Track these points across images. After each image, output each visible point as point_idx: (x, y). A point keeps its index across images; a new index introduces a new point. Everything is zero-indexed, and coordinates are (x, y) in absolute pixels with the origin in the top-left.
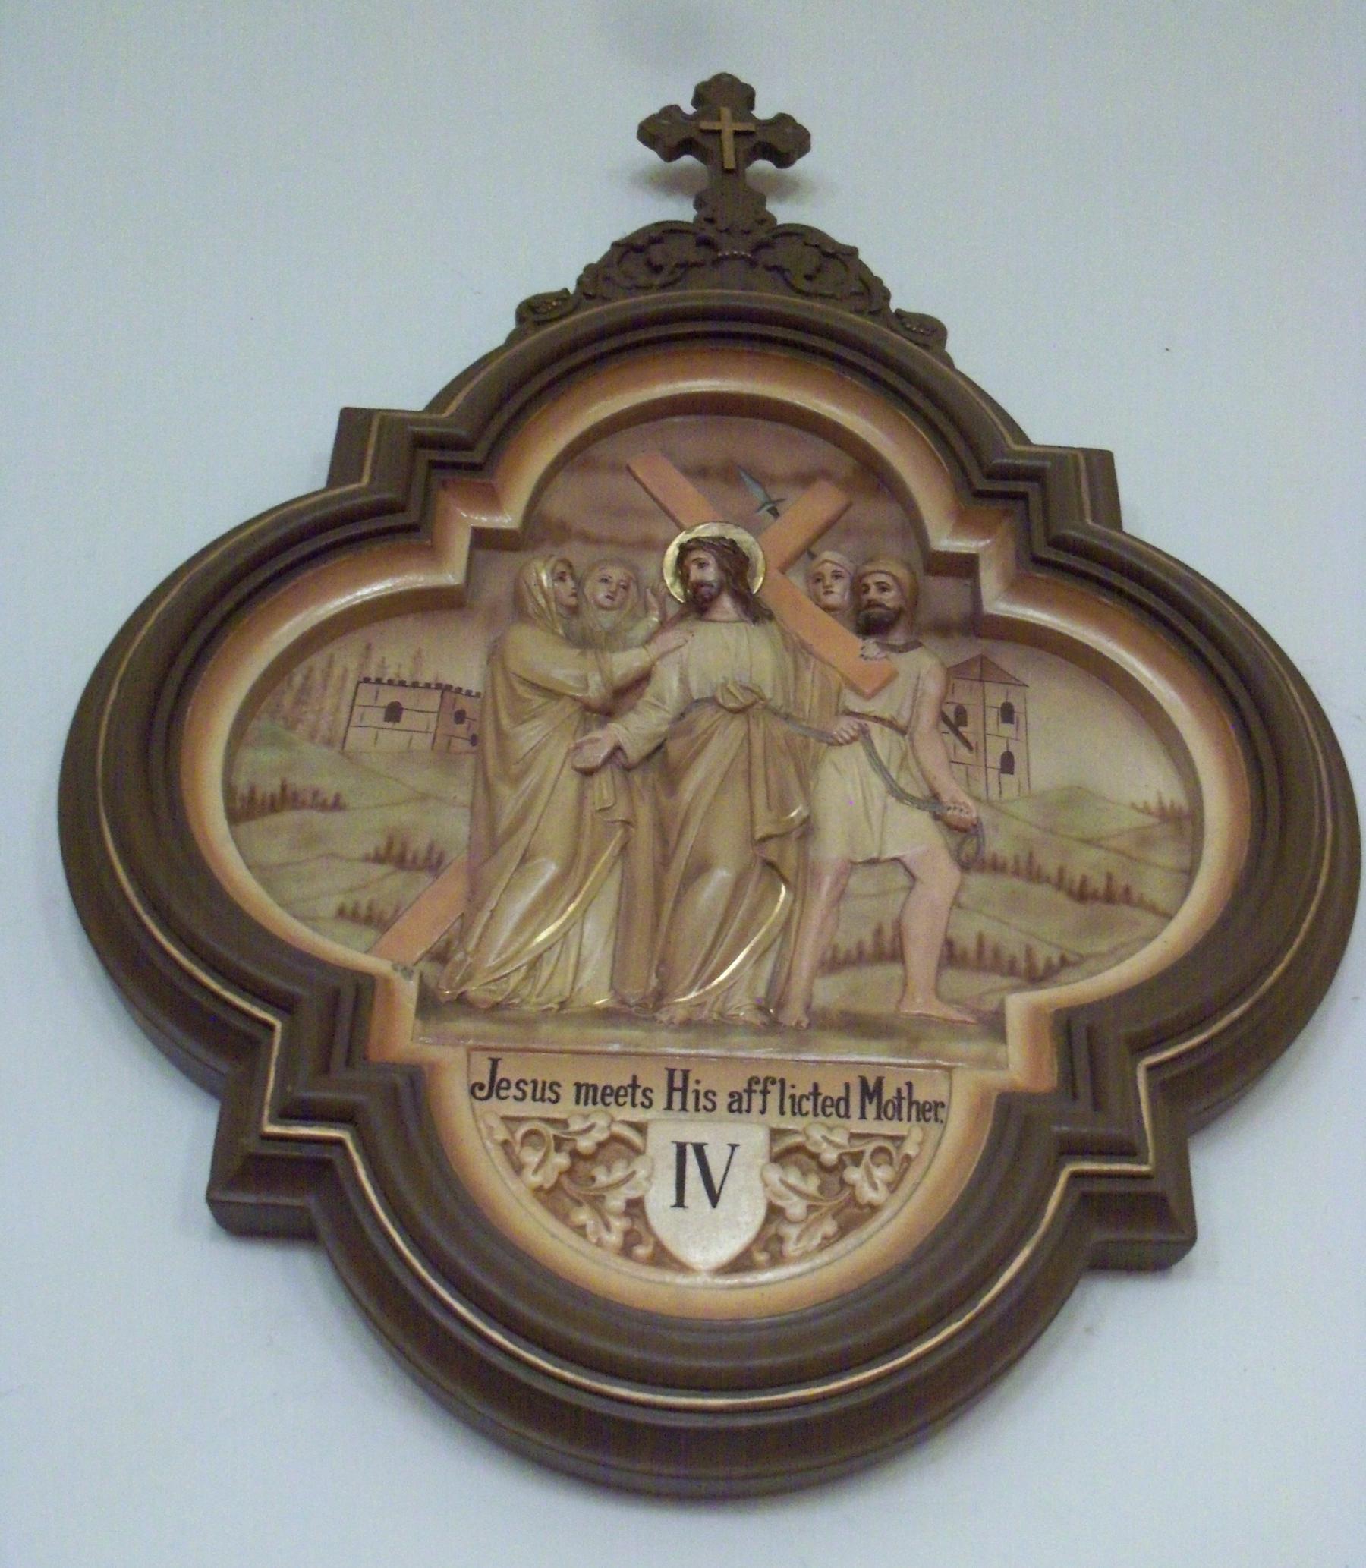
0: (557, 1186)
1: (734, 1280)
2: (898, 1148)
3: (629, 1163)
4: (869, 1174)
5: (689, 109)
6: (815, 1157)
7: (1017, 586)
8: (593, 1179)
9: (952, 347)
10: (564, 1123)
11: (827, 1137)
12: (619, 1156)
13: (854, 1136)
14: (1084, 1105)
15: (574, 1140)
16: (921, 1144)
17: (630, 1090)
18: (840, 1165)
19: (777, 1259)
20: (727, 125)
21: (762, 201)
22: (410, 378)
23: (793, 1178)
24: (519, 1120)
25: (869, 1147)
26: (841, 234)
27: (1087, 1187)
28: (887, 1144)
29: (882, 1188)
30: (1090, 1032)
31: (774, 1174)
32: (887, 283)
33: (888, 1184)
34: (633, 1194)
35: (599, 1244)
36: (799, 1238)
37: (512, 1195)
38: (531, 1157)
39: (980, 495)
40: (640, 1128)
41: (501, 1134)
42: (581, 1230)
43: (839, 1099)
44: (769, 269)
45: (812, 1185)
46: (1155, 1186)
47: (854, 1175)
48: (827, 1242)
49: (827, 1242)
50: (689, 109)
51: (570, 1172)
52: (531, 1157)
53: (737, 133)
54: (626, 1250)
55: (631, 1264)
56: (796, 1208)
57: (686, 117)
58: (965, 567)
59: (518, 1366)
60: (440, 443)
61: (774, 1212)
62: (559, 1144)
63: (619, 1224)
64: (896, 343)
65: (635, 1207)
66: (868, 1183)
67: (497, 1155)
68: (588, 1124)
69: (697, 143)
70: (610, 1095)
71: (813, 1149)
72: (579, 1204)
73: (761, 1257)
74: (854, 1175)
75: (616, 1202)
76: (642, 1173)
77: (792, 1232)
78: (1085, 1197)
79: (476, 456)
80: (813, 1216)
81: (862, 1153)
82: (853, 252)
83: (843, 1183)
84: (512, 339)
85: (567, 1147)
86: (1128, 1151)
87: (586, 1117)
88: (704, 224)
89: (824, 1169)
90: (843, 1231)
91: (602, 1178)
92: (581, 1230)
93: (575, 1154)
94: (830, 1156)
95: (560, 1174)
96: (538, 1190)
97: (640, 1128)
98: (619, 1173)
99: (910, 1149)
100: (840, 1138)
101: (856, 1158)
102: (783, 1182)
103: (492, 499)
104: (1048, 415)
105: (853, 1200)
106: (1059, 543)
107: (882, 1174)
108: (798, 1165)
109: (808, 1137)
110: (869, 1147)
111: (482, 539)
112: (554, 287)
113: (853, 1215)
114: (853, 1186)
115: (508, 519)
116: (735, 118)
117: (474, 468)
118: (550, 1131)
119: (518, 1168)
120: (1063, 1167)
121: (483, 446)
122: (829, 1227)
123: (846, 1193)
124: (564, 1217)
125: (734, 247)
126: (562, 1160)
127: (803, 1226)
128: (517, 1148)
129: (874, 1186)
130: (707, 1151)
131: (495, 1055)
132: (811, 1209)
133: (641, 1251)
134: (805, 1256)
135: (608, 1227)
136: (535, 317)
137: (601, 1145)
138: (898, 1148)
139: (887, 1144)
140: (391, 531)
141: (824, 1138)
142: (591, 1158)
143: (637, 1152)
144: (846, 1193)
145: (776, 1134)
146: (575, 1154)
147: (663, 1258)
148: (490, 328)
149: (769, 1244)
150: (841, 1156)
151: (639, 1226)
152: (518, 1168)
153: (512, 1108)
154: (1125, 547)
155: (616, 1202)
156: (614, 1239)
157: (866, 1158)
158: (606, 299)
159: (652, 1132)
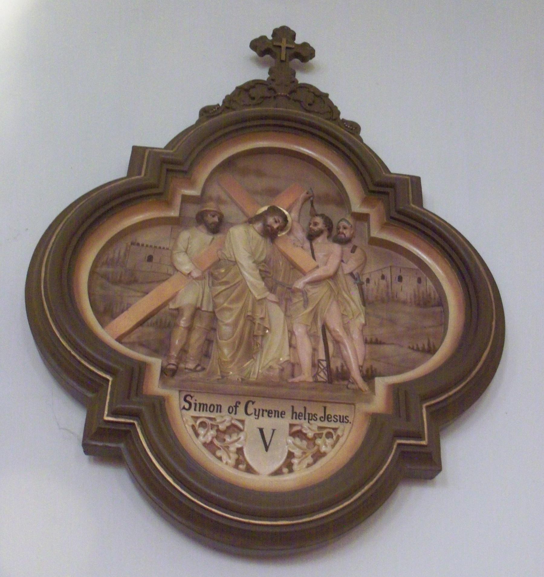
0: (212, 442)
2: (335, 432)
5: (270, 38)
6: (305, 435)
7: (384, 227)
8: (224, 440)
9: (362, 134)
12: (234, 432)
13: (320, 428)
15: (218, 426)
17: (234, 408)
18: (315, 437)
19: (291, 471)
20: (284, 44)
21: (294, 74)
23: (298, 441)
25: (325, 432)
27: (406, 449)
28: (331, 431)
29: (329, 447)
30: (406, 392)
31: (290, 440)
32: (339, 108)
33: (332, 446)
34: (239, 446)
35: (227, 463)
36: (299, 463)
38: (202, 431)
40: (242, 422)
42: (220, 459)
44: (295, 101)
47: (319, 441)
48: (309, 465)
49: (309, 465)
50: (270, 38)
51: (217, 437)
52: (202, 431)
53: (287, 48)
54: (236, 466)
55: (237, 470)
56: (297, 452)
57: (269, 40)
59: (198, 508)
60: (172, 162)
61: (291, 455)
62: (212, 426)
63: (234, 456)
64: (341, 132)
65: (240, 451)
66: (324, 445)
68: (223, 419)
69: (272, 51)
71: (304, 431)
72: (219, 449)
73: (285, 470)
76: (242, 438)
77: (295, 461)
78: (403, 452)
79: (185, 168)
80: (304, 456)
81: (322, 434)
83: (315, 444)
86: (420, 437)
87: (222, 417)
89: (308, 439)
90: (315, 462)
91: (228, 440)
92: (220, 459)
93: (218, 430)
95: (213, 438)
96: (205, 444)
98: (235, 437)
99: (339, 432)
100: (315, 428)
101: (320, 436)
103: (192, 184)
105: (319, 451)
107: (329, 441)
108: (298, 436)
110: (325, 432)
111: (186, 199)
113: (318, 456)
114: (319, 446)
115: (195, 192)
116: (287, 42)
117: (185, 172)
118: (209, 422)
119: (197, 435)
121: (189, 163)
122: (310, 460)
123: (316, 448)
124: (214, 454)
126: (213, 432)
127: (300, 460)
128: (197, 428)
129: (326, 446)
130: (264, 431)
132: (304, 453)
133: (241, 466)
137: (228, 428)
139: (331, 431)
141: (309, 428)
142: (224, 432)
143: (241, 430)
144: (316, 448)
145: (291, 426)
146: (218, 430)
147: (249, 470)
149: (289, 465)
151: (241, 458)
152: (197, 435)
154: (424, 214)
155: (233, 449)
156: (232, 462)
157: (324, 436)
158: (234, 110)
159: (246, 423)
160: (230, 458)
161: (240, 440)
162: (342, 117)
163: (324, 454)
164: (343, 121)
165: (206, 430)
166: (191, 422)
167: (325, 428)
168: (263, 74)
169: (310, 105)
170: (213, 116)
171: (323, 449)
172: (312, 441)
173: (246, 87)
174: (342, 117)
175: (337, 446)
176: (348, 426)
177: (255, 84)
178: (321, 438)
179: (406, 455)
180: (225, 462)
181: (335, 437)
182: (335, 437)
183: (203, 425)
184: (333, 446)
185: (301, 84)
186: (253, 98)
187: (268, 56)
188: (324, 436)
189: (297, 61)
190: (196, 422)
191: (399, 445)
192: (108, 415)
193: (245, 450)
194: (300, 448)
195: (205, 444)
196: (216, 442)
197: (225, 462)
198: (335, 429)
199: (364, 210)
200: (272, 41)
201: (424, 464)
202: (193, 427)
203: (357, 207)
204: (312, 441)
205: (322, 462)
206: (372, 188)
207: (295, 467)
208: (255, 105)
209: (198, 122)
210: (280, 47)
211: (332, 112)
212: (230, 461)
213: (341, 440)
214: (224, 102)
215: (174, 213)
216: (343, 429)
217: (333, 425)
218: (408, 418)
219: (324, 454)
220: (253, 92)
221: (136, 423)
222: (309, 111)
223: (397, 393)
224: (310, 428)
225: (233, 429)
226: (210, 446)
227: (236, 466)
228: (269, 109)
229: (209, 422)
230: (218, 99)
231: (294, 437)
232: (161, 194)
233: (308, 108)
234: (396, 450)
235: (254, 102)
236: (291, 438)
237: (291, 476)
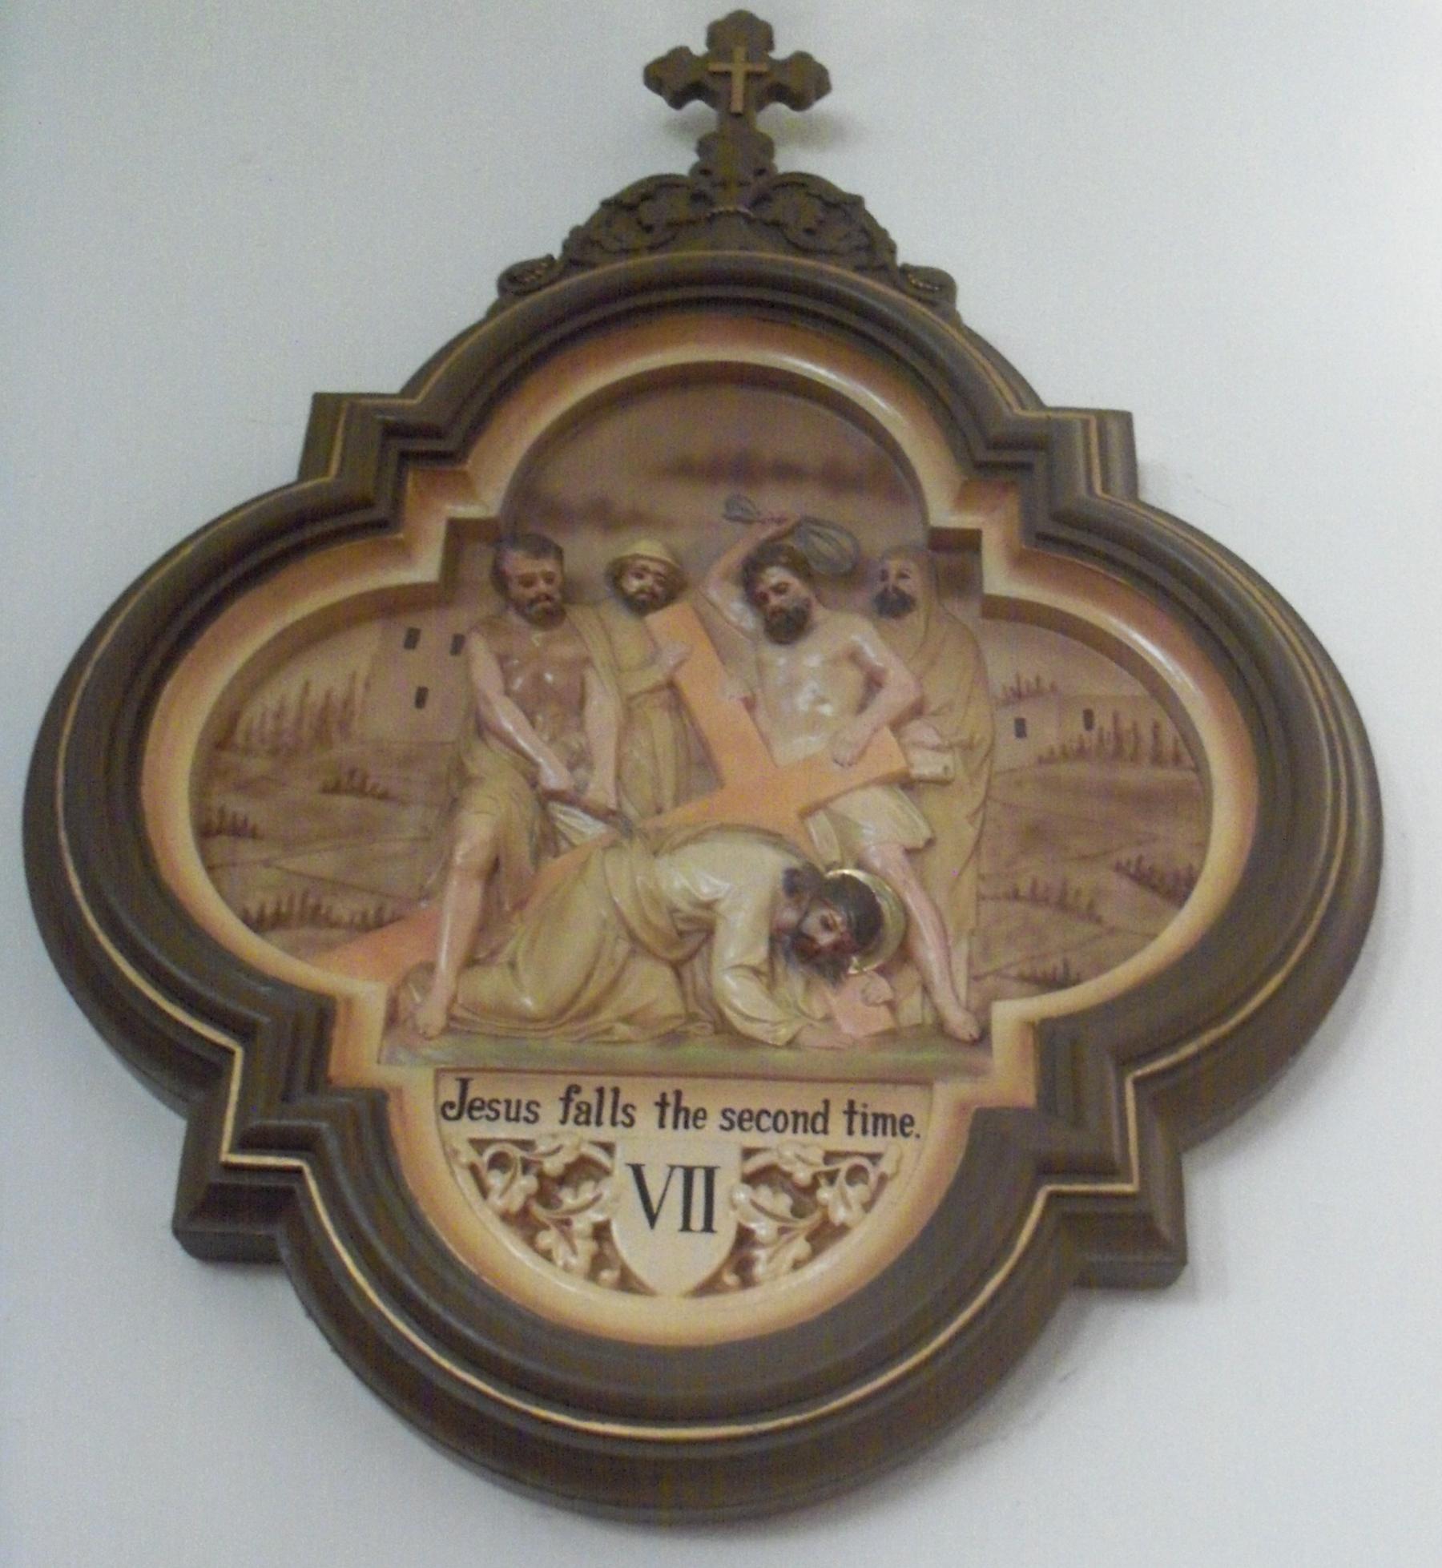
0: (525, 1211)
3: (597, 1180)
6: (788, 1176)
10: (526, 1145)
11: (798, 1153)
13: (829, 1157)
15: (540, 1163)
16: (899, 1161)
22: (384, 360)
23: (764, 1196)
25: (844, 1166)
28: (865, 1162)
29: (856, 1207)
31: (743, 1194)
35: (566, 1268)
36: (770, 1259)
37: (475, 1224)
38: (495, 1180)
40: (608, 1148)
42: (547, 1255)
43: (817, 1114)
45: (783, 1203)
49: (797, 1265)
54: (593, 1273)
56: (763, 1229)
61: (744, 1238)
62: (526, 1167)
65: (601, 1232)
68: (555, 1145)
70: (750, 1120)
71: (786, 1168)
72: (546, 1227)
73: (730, 1279)
75: (582, 1224)
77: (761, 1254)
80: (785, 1237)
81: (837, 1171)
82: (857, 202)
85: (534, 1170)
88: (701, 177)
90: (816, 1252)
93: (541, 1176)
94: (803, 1175)
95: (529, 1197)
98: (587, 1191)
99: (886, 1166)
100: (816, 1156)
101: (831, 1177)
102: (754, 1204)
105: (826, 1222)
108: (771, 1184)
109: (781, 1156)
110: (844, 1166)
112: (537, 253)
113: (825, 1235)
118: (517, 1153)
119: (484, 1191)
122: (800, 1247)
124: (531, 1242)
125: (729, 203)
128: (483, 1170)
129: (848, 1205)
131: (465, 1075)
132: (782, 1231)
133: (606, 1275)
135: (574, 1252)
136: (516, 288)
139: (865, 1162)
141: (798, 1157)
146: (541, 1176)
147: (627, 1283)
148: (467, 300)
150: (815, 1178)
151: (608, 1252)
152: (484, 1191)
153: (481, 1129)
155: (582, 1224)
156: (581, 1261)
157: (842, 1176)
160: (574, 1252)
161: (601, 1202)
163: (843, 1230)
164: (906, 270)
165: (509, 1175)
166: (468, 1155)
168: (680, 160)
169: (809, 231)
171: (840, 1215)
172: (804, 1195)
173: (627, 200)
176: (907, 1145)
177: (657, 188)
180: (560, 1263)
181: (873, 1178)
182: (873, 1178)
183: (499, 1162)
184: (868, 1206)
185: (785, 175)
186: (649, 229)
187: (697, 106)
188: (842, 1176)
189: (779, 110)
190: (480, 1153)
192: (232, 1150)
193: (615, 1229)
194: (773, 1216)
195: (506, 1217)
196: (538, 1211)
197: (560, 1263)
198: (874, 1158)
199: (966, 520)
200: (705, 59)
201: (1138, 1249)
202: (473, 1169)
203: (944, 513)
204: (804, 1195)
206: (983, 455)
207: (759, 1270)
208: (652, 249)
209: (494, 311)
211: (872, 245)
212: (573, 1261)
213: (891, 1192)
215: (425, 568)
217: (870, 1144)
219: (843, 1230)
220: (647, 213)
221: (307, 1170)
222: (806, 252)
223: (1052, 1041)
224: (798, 1153)
225: (582, 1169)
226: (523, 1222)
227: (593, 1273)
228: (692, 255)
229: (517, 1153)
232: (382, 525)
233: (804, 240)
236: (746, 1187)
237: (752, 1296)
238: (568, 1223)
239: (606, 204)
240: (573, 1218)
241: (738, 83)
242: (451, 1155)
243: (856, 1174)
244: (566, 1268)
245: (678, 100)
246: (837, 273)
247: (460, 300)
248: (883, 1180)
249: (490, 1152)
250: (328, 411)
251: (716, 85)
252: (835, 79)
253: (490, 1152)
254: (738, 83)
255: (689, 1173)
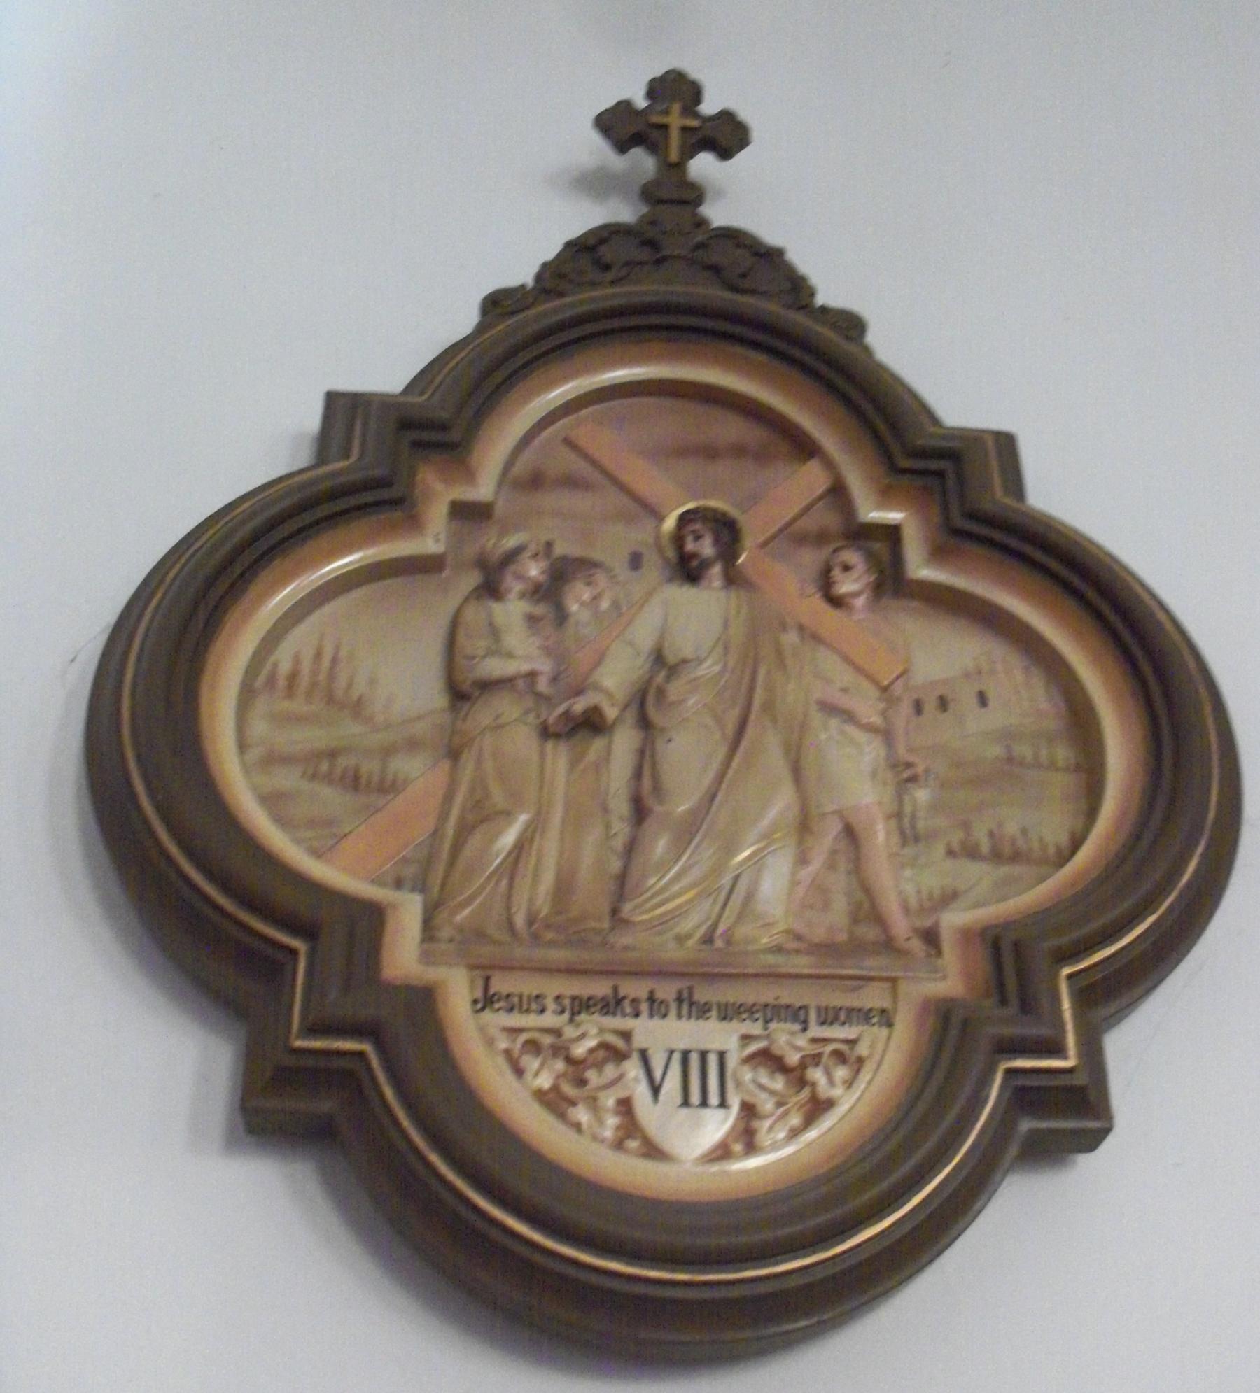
0: (555, 1088)
1: (715, 1168)
4: (828, 1073)
7: (938, 553)
10: (557, 1033)
11: (790, 1041)
13: (814, 1041)
14: (1013, 1009)
15: (567, 1049)
18: (803, 1065)
19: (751, 1147)
23: (764, 1077)
24: (520, 1030)
25: (829, 1048)
26: (770, 236)
31: (747, 1075)
33: (845, 1082)
34: (622, 1093)
35: (595, 1138)
36: (771, 1129)
39: (904, 471)
41: (503, 1044)
45: (779, 1083)
46: (1080, 1080)
49: (794, 1133)
54: (619, 1145)
58: (893, 533)
61: (749, 1110)
63: (612, 1121)
65: (626, 1106)
67: (501, 1061)
71: (776, 1051)
72: (573, 1103)
73: (738, 1147)
74: (816, 1075)
80: (782, 1109)
81: (819, 1055)
84: (480, 329)
86: (1056, 1049)
92: (577, 1127)
93: (569, 1060)
94: (793, 1059)
95: (558, 1077)
96: (540, 1095)
97: (626, 1035)
99: (862, 1049)
101: (816, 1059)
104: (958, 401)
106: (973, 516)
107: (841, 1073)
109: (772, 1042)
110: (829, 1048)
113: (818, 1107)
114: (814, 1085)
118: (547, 1040)
119: (519, 1072)
120: (999, 1061)
122: (795, 1120)
124: (562, 1116)
132: (779, 1104)
133: (633, 1144)
134: (775, 1147)
135: (601, 1122)
137: (592, 1051)
138: (852, 1049)
140: (378, 504)
145: (746, 1039)
146: (569, 1060)
152: (519, 1072)
155: (609, 1100)
156: (608, 1133)
157: (825, 1059)
158: (561, 294)
162: (820, 300)
163: (829, 1104)
167: (825, 1041)
170: (513, 313)
171: (824, 1089)
173: (592, 242)
174: (820, 300)
175: (861, 1085)
178: (817, 1065)
179: (1027, 1096)
183: (533, 1047)
184: (849, 1084)
190: (514, 1041)
191: (1010, 1072)
196: (568, 1089)
198: (852, 1043)
201: (1069, 1115)
204: (797, 1076)
205: (827, 1122)
210: (664, 127)
211: (798, 289)
214: (539, 277)
216: (870, 1038)
218: (1027, 1006)
220: (606, 253)
222: (743, 291)
224: (790, 1041)
226: (554, 1102)
227: (619, 1145)
228: (648, 288)
229: (547, 1040)
230: (523, 274)
231: (755, 1068)
234: (1003, 1087)
235: (610, 276)
236: (746, 1068)
238: (595, 1099)
239: (569, 245)
240: (601, 1095)
241: (675, 138)
242: (490, 1042)
243: (840, 1057)
244: (595, 1138)
245: (622, 146)
246: (771, 308)
247: (450, 319)
248: (860, 1061)
249: (524, 1037)
250: (343, 410)
251: (655, 135)
252: (755, 134)
253: (524, 1037)
254: (675, 138)
255: (685, 1055)
